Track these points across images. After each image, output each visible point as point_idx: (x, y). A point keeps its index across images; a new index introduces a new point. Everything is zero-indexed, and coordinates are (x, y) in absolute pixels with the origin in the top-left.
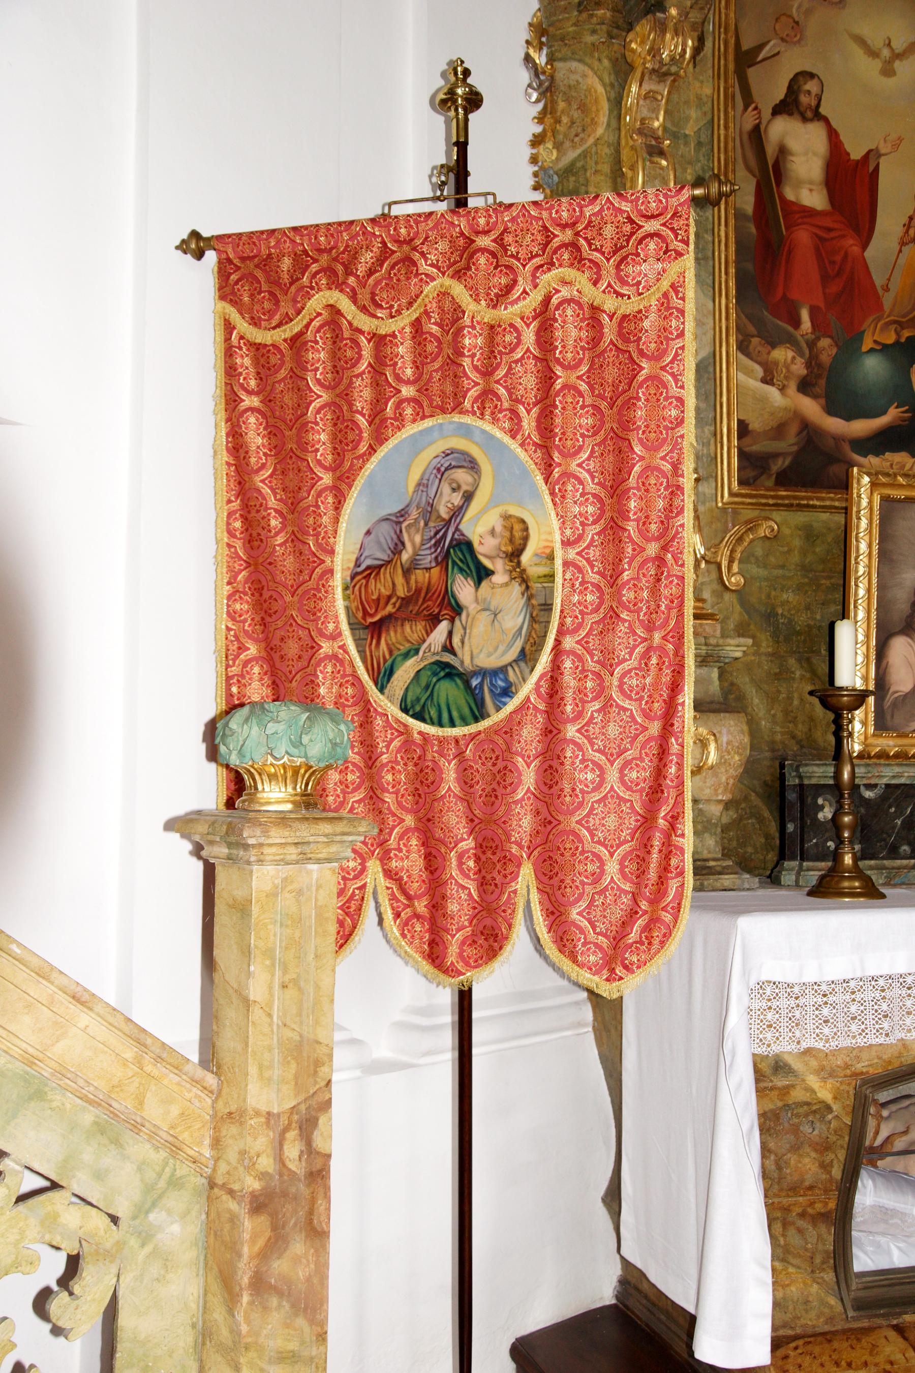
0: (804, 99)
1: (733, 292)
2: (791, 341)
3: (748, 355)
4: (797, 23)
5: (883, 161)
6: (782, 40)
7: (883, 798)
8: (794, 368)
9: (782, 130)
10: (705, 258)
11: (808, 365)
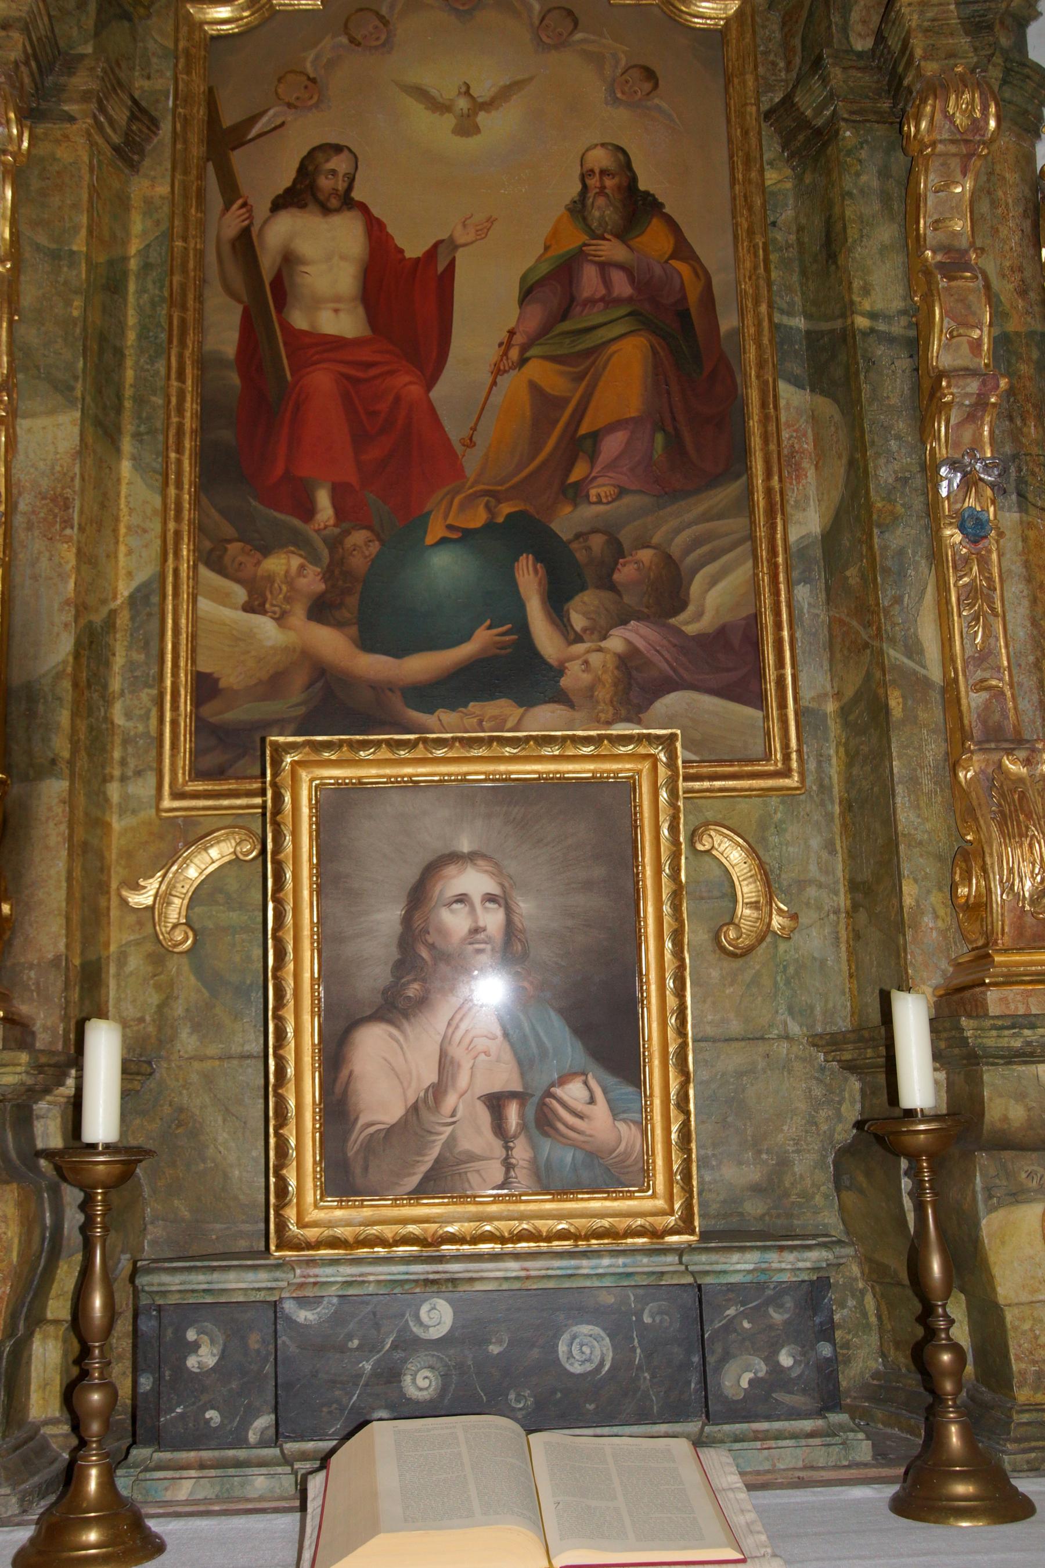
0: (325, 183)
2: (299, 542)
3: (220, 570)
4: (313, 81)
5: (460, 256)
6: (289, 105)
7: (337, 1319)
8: (302, 582)
9: (282, 231)
11: (328, 575)
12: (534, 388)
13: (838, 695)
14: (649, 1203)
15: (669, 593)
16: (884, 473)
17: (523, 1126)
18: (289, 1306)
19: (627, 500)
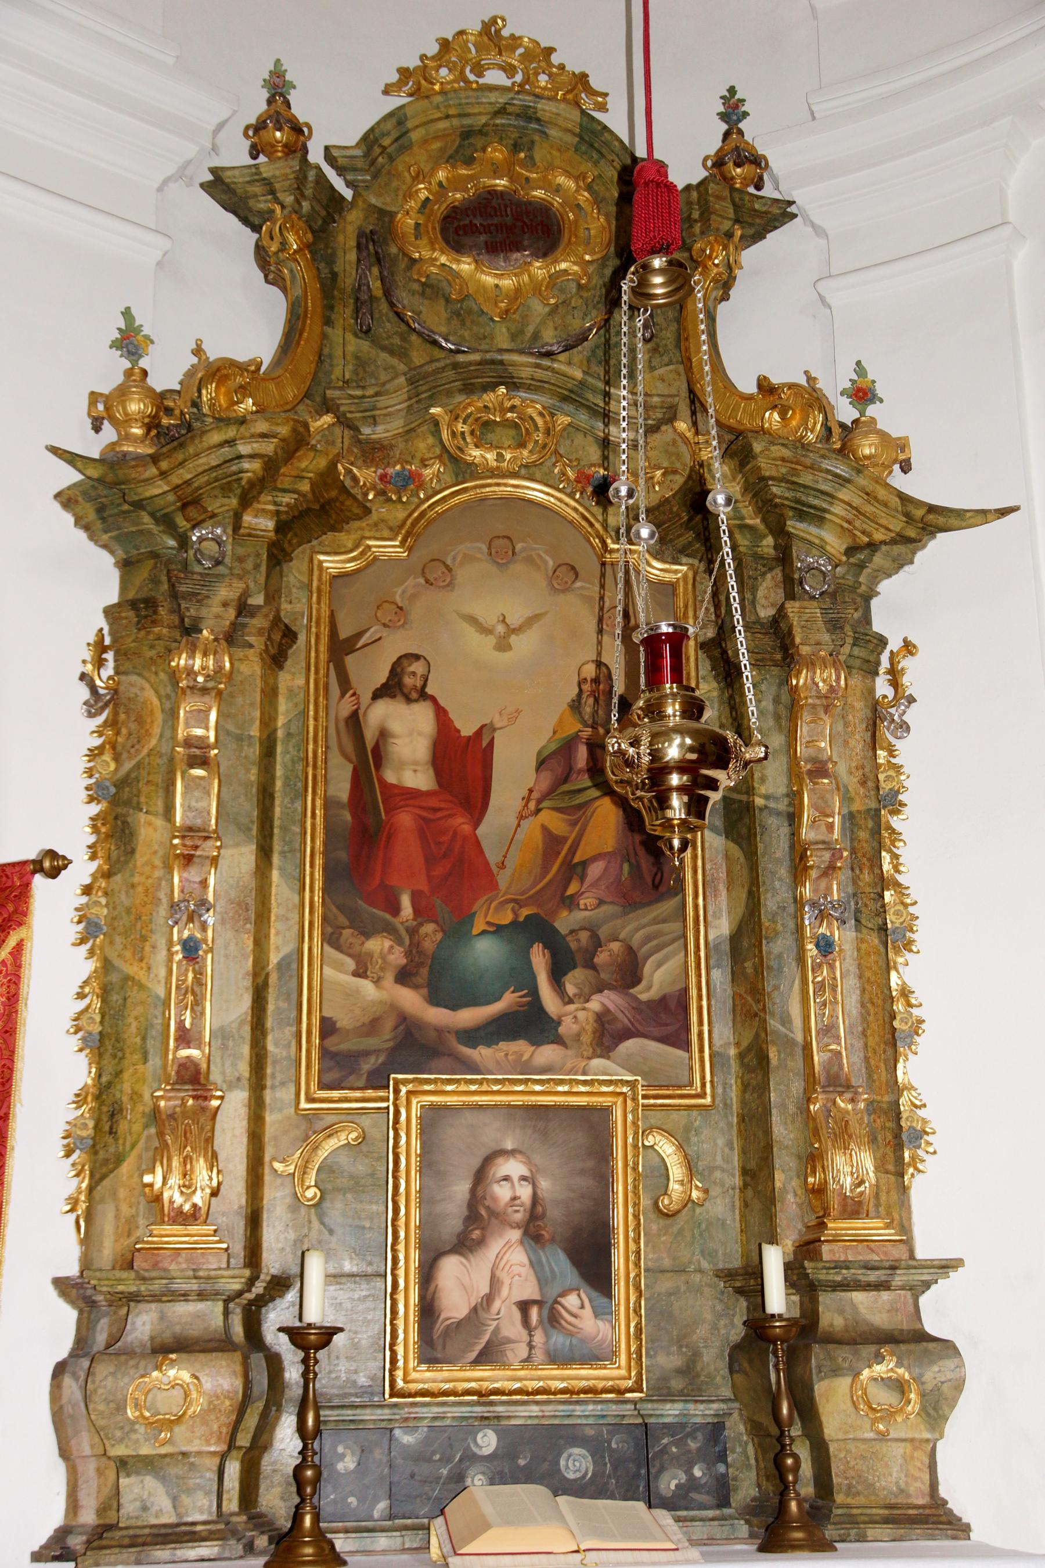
0: (408, 681)
1: (318, 884)
2: (389, 930)
3: (338, 948)
4: (401, 608)
5: (497, 735)
6: (385, 625)
7: (427, 1441)
8: (391, 958)
10: (292, 851)
11: (408, 954)
12: (545, 829)
13: (737, 1044)
14: (616, 1372)
15: (630, 972)
16: (770, 903)
17: (541, 1322)
18: (397, 1432)
19: (604, 908)
